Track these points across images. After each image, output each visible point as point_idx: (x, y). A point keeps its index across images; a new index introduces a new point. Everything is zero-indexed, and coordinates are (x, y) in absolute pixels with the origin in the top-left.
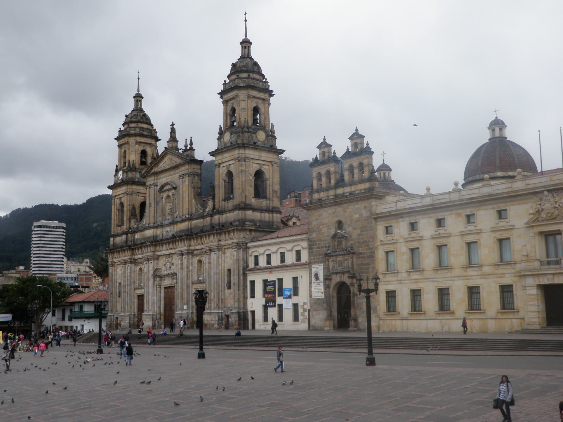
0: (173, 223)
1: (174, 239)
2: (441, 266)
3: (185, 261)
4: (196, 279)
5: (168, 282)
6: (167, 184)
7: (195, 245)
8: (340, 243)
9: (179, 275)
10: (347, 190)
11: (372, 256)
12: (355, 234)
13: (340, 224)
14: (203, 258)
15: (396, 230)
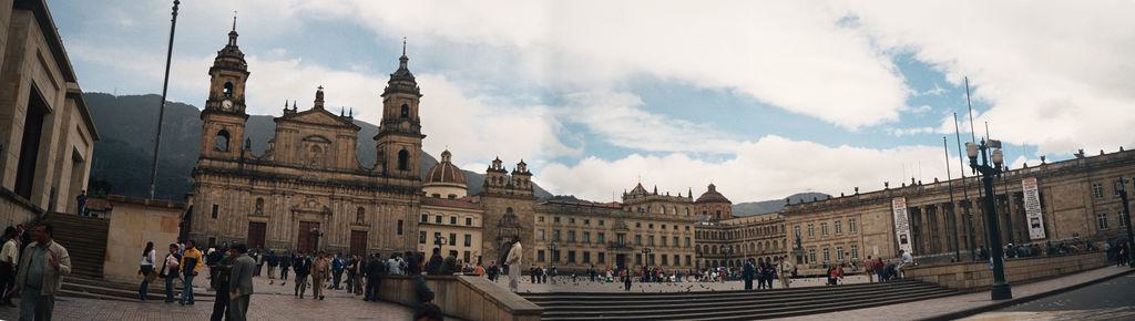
0: (325, 170)
1: (331, 184)
2: (664, 244)
3: (346, 206)
4: (354, 220)
5: (308, 217)
6: (319, 136)
7: (367, 196)
8: (509, 220)
9: (336, 215)
10: (515, 191)
11: (533, 230)
12: (521, 217)
13: (510, 210)
14: (367, 207)
15: (546, 220)
